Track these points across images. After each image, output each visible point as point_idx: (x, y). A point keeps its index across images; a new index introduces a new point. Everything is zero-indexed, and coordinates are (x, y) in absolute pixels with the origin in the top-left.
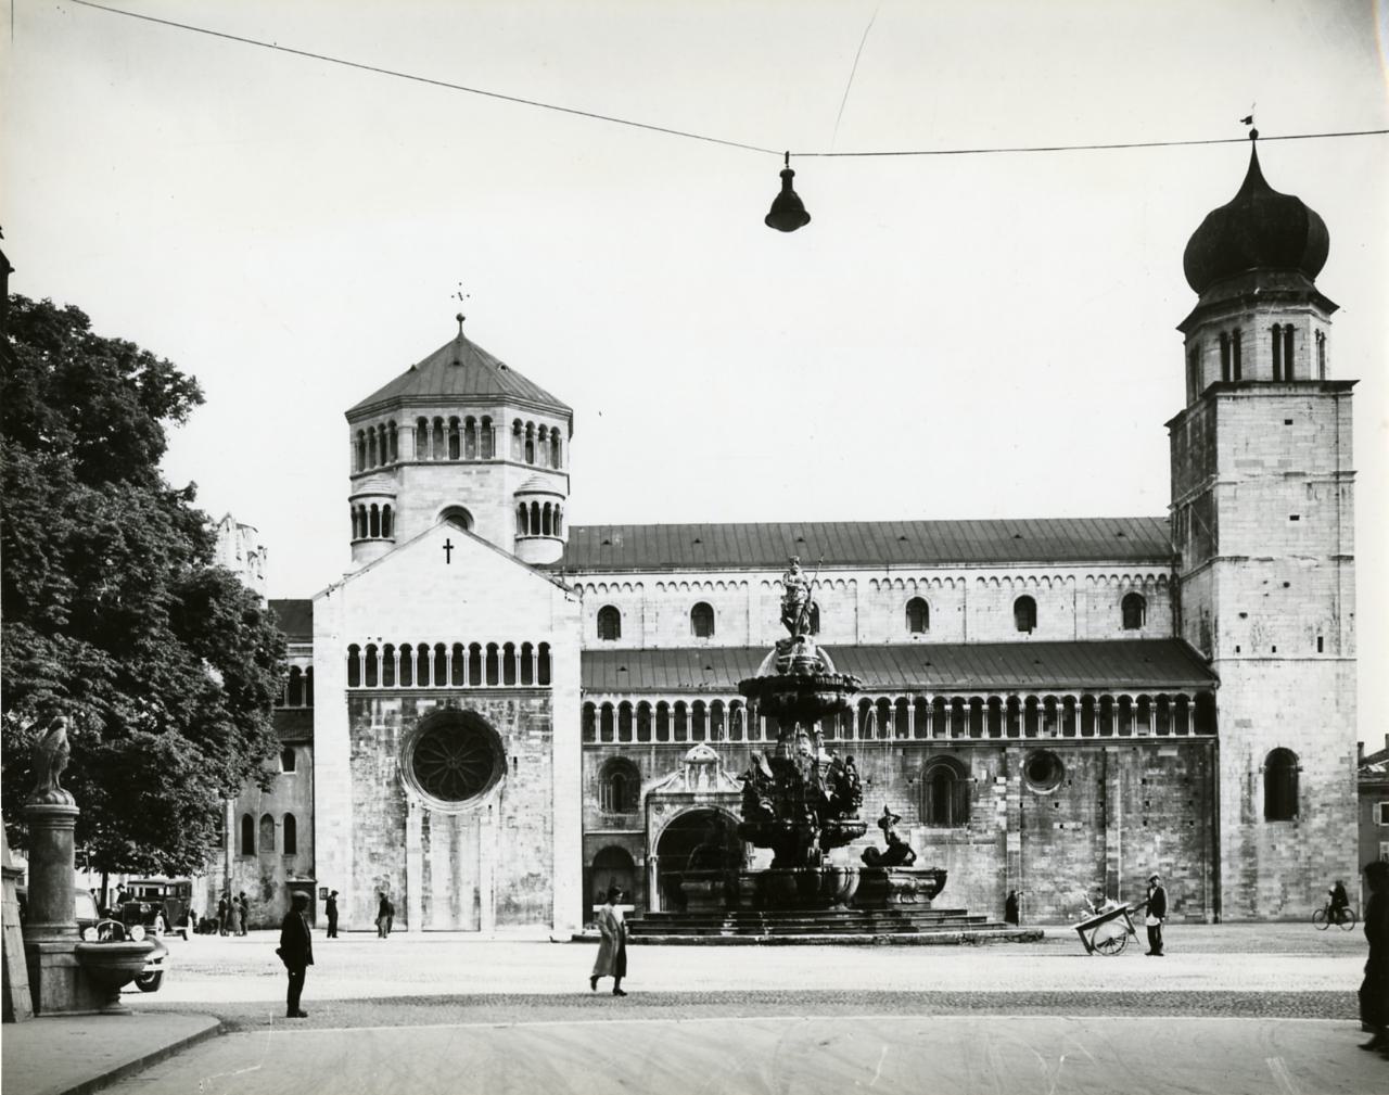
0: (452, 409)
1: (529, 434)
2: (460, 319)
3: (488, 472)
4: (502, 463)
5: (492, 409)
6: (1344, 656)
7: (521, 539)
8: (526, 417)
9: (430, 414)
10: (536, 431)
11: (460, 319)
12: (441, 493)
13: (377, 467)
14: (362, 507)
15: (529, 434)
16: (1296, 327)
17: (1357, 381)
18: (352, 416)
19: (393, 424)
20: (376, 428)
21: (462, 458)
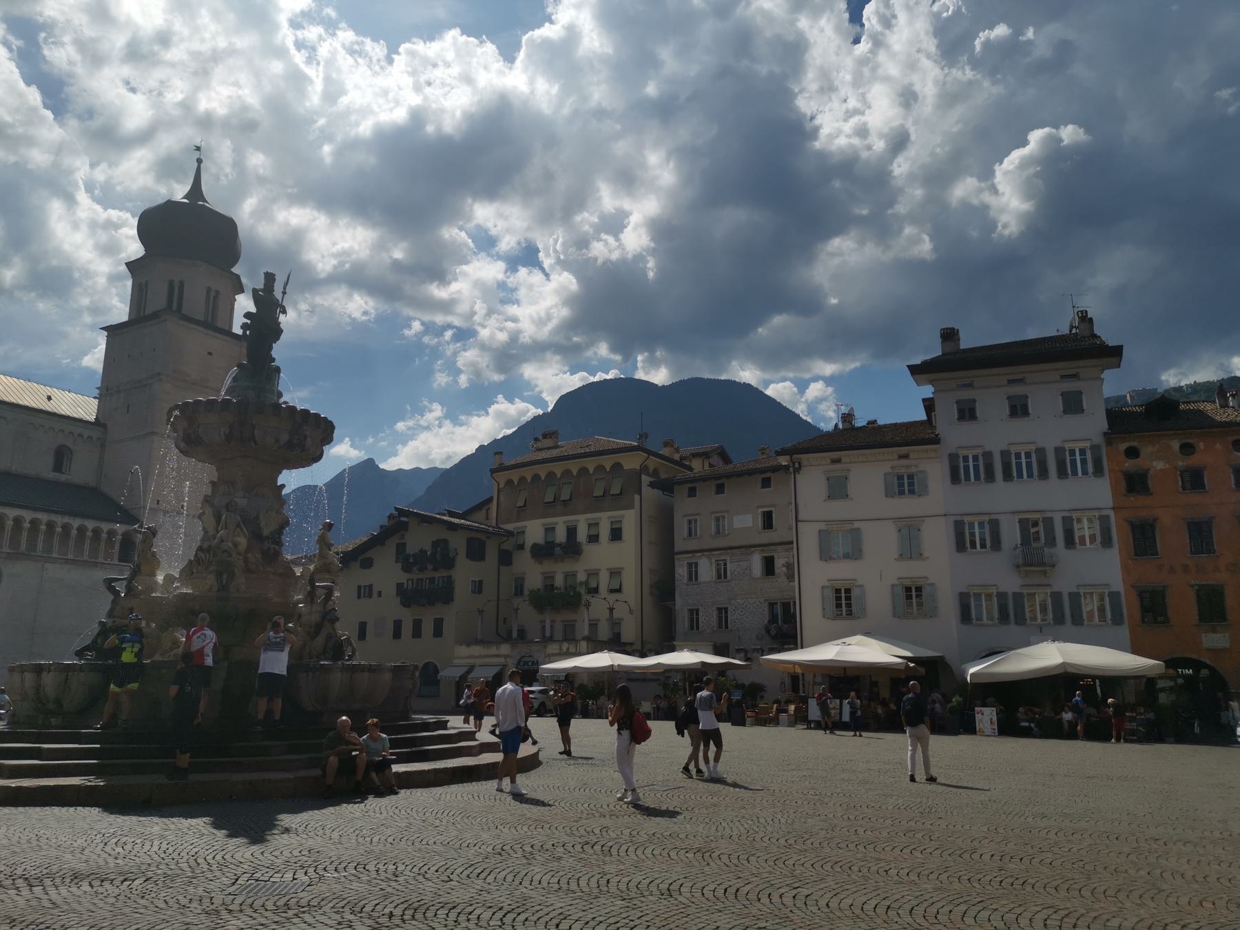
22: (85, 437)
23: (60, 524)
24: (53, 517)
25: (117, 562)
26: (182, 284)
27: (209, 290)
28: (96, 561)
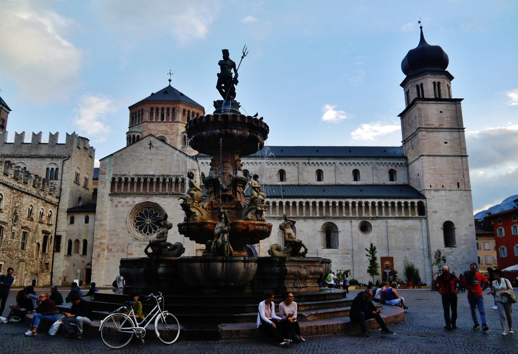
0: (162, 105)
1: (189, 114)
2: (170, 80)
3: (173, 125)
4: (178, 122)
5: (176, 105)
6: (467, 189)
7: (184, 147)
8: (187, 108)
9: (155, 106)
10: (191, 114)
11: (170, 80)
12: (157, 132)
13: (137, 123)
14: (130, 136)
15: (189, 114)
16: (441, 82)
17: (462, 99)
18: (130, 108)
19: (142, 110)
20: (137, 111)
21: (164, 121)
22: (399, 164)
23: (390, 203)
24: (387, 200)
25: (417, 216)
26: (422, 84)
27: (434, 83)
28: (408, 216)
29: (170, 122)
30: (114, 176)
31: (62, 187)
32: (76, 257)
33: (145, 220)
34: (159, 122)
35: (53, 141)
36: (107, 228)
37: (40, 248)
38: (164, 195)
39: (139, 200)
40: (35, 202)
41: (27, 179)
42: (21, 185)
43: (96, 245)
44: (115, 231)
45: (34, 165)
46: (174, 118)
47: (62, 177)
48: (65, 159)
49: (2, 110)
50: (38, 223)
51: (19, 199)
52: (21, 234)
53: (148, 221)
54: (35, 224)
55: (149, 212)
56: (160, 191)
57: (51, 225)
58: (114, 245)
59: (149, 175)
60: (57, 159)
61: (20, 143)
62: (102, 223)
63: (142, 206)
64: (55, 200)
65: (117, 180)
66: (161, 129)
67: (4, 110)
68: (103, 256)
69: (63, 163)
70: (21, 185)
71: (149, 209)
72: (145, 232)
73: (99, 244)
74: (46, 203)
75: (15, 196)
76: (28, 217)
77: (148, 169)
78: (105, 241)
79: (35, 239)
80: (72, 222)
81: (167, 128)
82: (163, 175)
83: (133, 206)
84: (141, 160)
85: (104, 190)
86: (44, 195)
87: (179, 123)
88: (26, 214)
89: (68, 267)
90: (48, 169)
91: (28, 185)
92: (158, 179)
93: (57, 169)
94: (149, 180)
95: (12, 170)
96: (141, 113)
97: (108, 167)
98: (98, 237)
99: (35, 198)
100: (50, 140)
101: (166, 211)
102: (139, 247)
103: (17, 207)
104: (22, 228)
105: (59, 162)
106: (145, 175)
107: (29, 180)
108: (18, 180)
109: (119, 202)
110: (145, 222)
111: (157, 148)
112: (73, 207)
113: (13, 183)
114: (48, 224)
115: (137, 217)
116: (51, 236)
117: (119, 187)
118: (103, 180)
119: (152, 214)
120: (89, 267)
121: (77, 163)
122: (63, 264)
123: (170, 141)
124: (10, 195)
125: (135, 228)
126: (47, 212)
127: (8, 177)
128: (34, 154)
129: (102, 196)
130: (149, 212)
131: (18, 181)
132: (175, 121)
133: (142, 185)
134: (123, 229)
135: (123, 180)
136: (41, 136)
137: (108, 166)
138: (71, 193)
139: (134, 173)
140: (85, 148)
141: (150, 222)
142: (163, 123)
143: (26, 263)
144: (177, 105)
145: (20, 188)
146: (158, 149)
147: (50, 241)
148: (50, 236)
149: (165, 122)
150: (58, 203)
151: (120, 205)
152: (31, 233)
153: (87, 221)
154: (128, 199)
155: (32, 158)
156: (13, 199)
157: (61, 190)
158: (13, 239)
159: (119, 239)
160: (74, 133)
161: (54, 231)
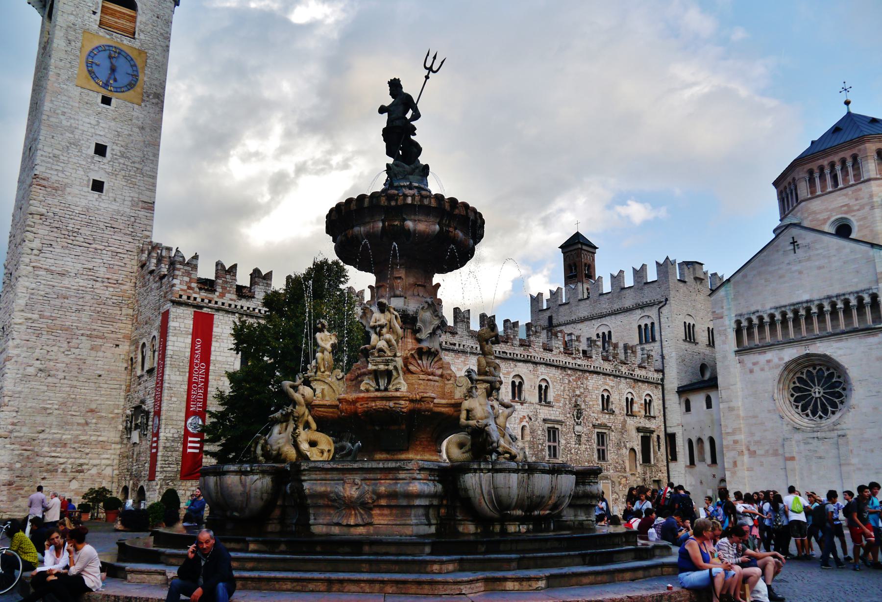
2: (847, 103)
3: (860, 190)
4: (869, 180)
5: (857, 148)
9: (814, 165)
11: (847, 103)
12: (829, 213)
18: (776, 184)
19: (794, 179)
21: (840, 186)
29: (852, 186)
30: (739, 318)
31: (664, 352)
32: (702, 468)
33: (810, 391)
34: (830, 192)
35: (639, 280)
36: (742, 413)
37: (638, 457)
38: (837, 335)
39: (791, 353)
40: (611, 383)
41: (591, 351)
42: (579, 362)
43: (727, 446)
44: (755, 417)
45: (620, 326)
46: (857, 176)
47: (661, 335)
48: (661, 305)
49: (583, 252)
50: (626, 417)
51: (579, 383)
52: (595, 436)
53: (817, 391)
54: (619, 418)
55: (815, 374)
56: (829, 329)
57: (654, 417)
58: (758, 443)
59: (802, 303)
60: (650, 308)
61: (598, 295)
62: (732, 404)
63: (799, 364)
64: (655, 376)
65: (745, 324)
66: (837, 206)
67: (585, 250)
68: (743, 465)
69: (660, 313)
70: (579, 362)
71: (828, 369)
72: (814, 414)
73: (732, 443)
74: (635, 382)
75: (571, 379)
76: (603, 409)
77: (797, 292)
78: (742, 437)
79: (624, 442)
80: (688, 409)
81: (847, 199)
82: (829, 297)
83: (782, 367)
84: (781, 277)
85: (727, 343)
86: (629, 370)
87: (872, 182)
88: (598, 405)
89: (694, 486)
90: (640, 326)
91: (593, 359)
92: (821, 307)
93: (653, 324)
94: (802, 312)
95: (559, 340)
96: (792, 187)
97: (725, 304)
98: (729, 430)
99: (611, 378)
100: (635, 281)
101: (846, 366)
102: (805, 443)
103: (579, 396)
104: (594, 426)
105: (653, 312)
106: (793, 305)
107: (594, 352)
108: (572, 354)
109: (754, 364)
110: (811, 395)
111: (808, 247)
112: (689, 383)
113: (563, 359)
114: (645, 416)
115: (792, 385)
116: (658, 437)
117: (750, 335)
118: (720, 329)
119: (823, 377)
120: (722, 485)
121: (685, 308)
122: (686, 481)
123: (858, 223)
124: (563, 379)
125: (794, 407)
126: (640, 397)
127: (553, 353)
128: (618, 307)
129: (725, 357)
130: (815, 374)
131: (574, 356)
132: (862, 179)
133: (791, 324)
134: (769, 411)
135: (756, 321)
136: (623, 277)
137: (725, 301)
138: (680, 360)
139: (773, 305)
140: (696, 279)
141: (822, 393)
142: (838, 193)
143: (613, 482)
144: (860, 147)
145: (579, 365)
146: (809, 248)
147: (656, 444)
148: (654, 436)
149: (841, 189)
150: (662, 380)
151: (756, 368)
152: (613, 433)
153: (709, 405)
154: (770, 355)
155: (616, 314)
156: (568, 384)
157: (663, 357)
158: (580, 444)
159: (765, 431)
160: (667, 258)
161: (663, 427)
